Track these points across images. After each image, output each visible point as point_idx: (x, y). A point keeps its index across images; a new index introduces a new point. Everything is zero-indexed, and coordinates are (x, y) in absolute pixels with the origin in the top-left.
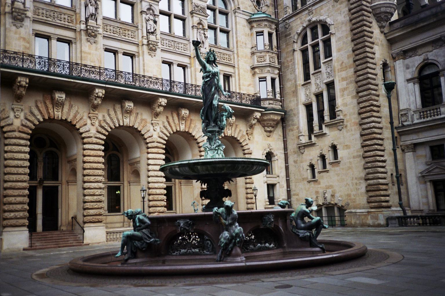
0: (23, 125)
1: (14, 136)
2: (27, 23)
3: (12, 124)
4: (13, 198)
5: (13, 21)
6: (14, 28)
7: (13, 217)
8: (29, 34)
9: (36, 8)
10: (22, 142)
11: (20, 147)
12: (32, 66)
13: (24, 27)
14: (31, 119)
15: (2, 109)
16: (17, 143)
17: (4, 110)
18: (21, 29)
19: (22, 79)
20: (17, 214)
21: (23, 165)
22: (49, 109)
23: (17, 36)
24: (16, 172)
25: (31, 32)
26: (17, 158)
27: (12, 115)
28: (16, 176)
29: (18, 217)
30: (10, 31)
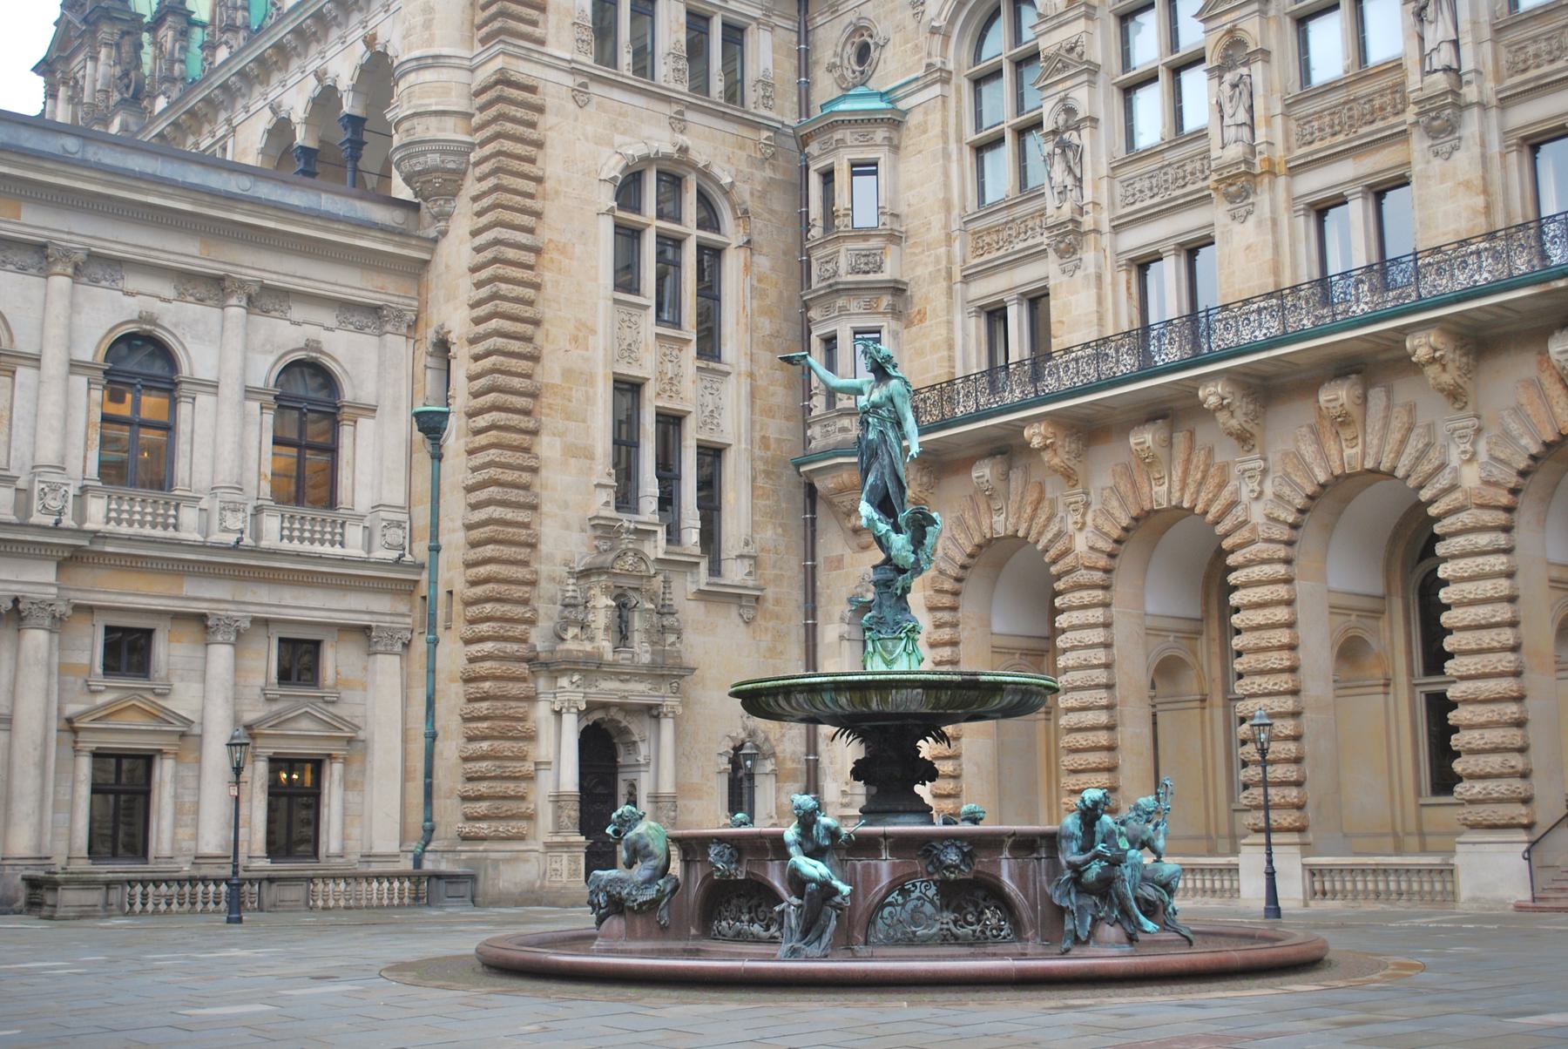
0: (1487, 483)
1: (1459, 525)
2: (1471, 124)
3: (1453, 487)
4: (1476, 734)
5: (1430, 142)
6: (1437, 163)
7: (1480, 797)
8: (1484, 159)
9: (1514, 48)
10: (1483, 540)
11: (1480, 560)
12: (1444, 281)
13: (1463, 144)
14: (1502, 456)
15: (1420, 446)
16: (1469, 548)
17: (1428, 445)
18: (1457, 155)
19: (1416, 342)
20: (1491, 785)
21: (1493, 620)
22: (1554, 402)
23: (1449, 184)
24: (1474, 646)
25: (1495, 147)
26: (1472, 596)
27: (1455, 458)
28: (1477, 658)
29: (1495, 795)
30: (1428, 178)
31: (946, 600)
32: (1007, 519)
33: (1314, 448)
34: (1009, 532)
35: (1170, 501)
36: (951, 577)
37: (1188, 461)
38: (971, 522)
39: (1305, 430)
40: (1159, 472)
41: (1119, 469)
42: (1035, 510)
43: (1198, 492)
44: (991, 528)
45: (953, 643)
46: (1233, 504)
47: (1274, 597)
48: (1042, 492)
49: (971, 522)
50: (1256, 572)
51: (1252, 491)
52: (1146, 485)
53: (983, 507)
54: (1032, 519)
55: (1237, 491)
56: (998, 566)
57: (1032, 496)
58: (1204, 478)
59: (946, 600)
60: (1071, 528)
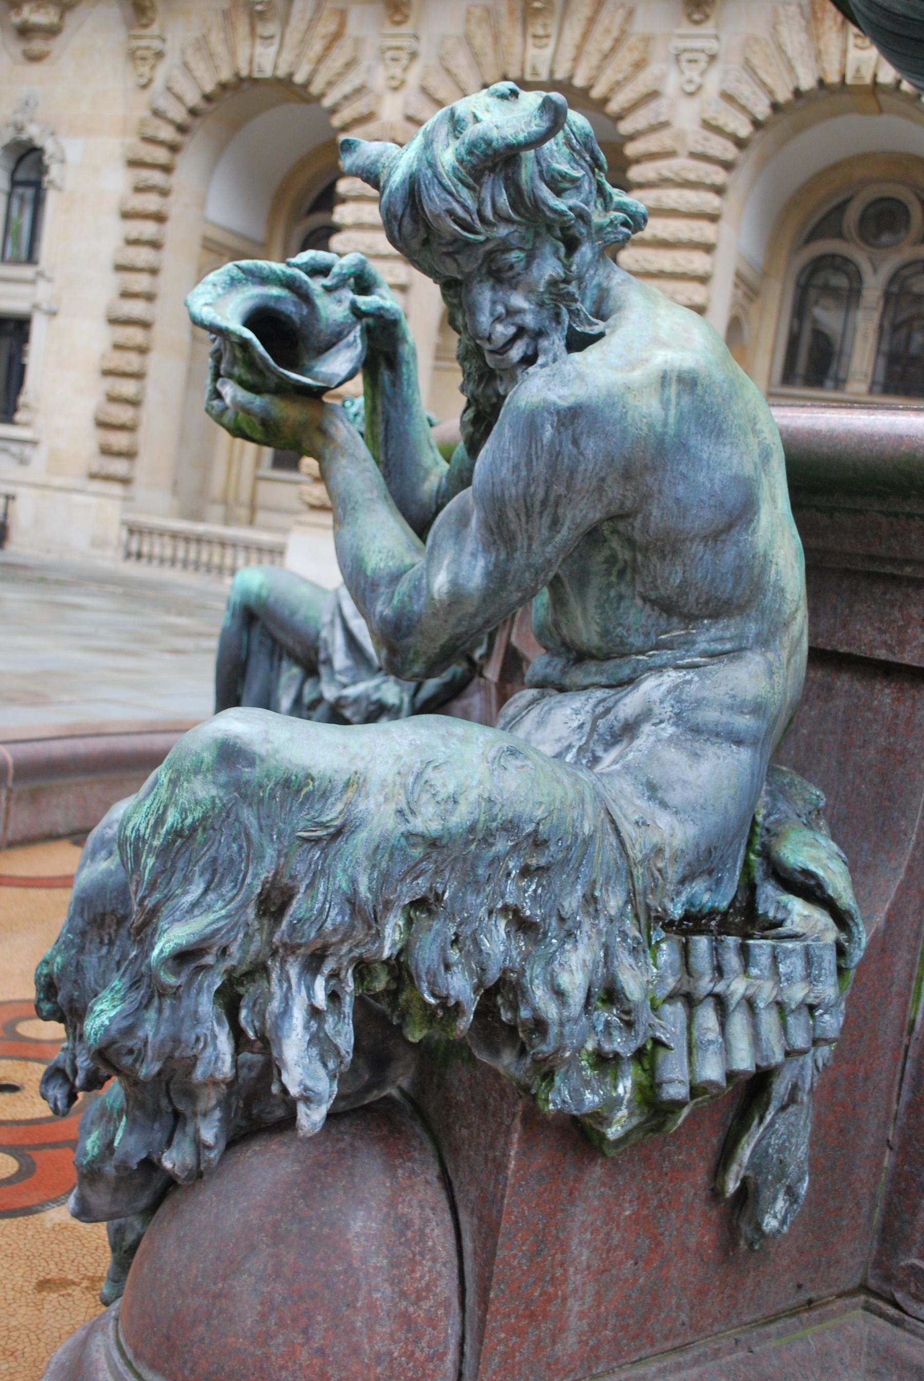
31: (161, 155)
32: (279, 53)
33: (802, 37)
34: (282, 72)
35: (552, 72)
36: (171, 122)
37: (592, 21)
38: (219, 48)
39: (793, 10)
40: (545, 26)
41: (478, 12)
42: (328, 48)
43: (600, 68)
44: (251, 62)
45: (160, 218)
46: (653, 95)
47: (696, 236)
48: (342, 25)
49: (219, 48)
50: (672, 197)
51: (690, 81)
52: (518, 39)
53: (243, 28)
54: (320, 60)
55: (662, 78)
56: (235, 125)
57: (327, 27)
58: (613, 49)
59: (161, 155)
60: (379, 80)
